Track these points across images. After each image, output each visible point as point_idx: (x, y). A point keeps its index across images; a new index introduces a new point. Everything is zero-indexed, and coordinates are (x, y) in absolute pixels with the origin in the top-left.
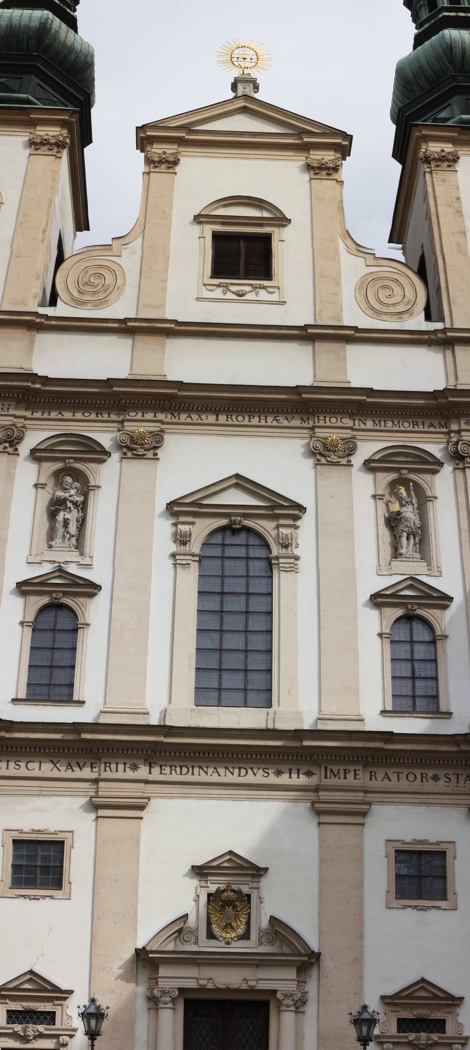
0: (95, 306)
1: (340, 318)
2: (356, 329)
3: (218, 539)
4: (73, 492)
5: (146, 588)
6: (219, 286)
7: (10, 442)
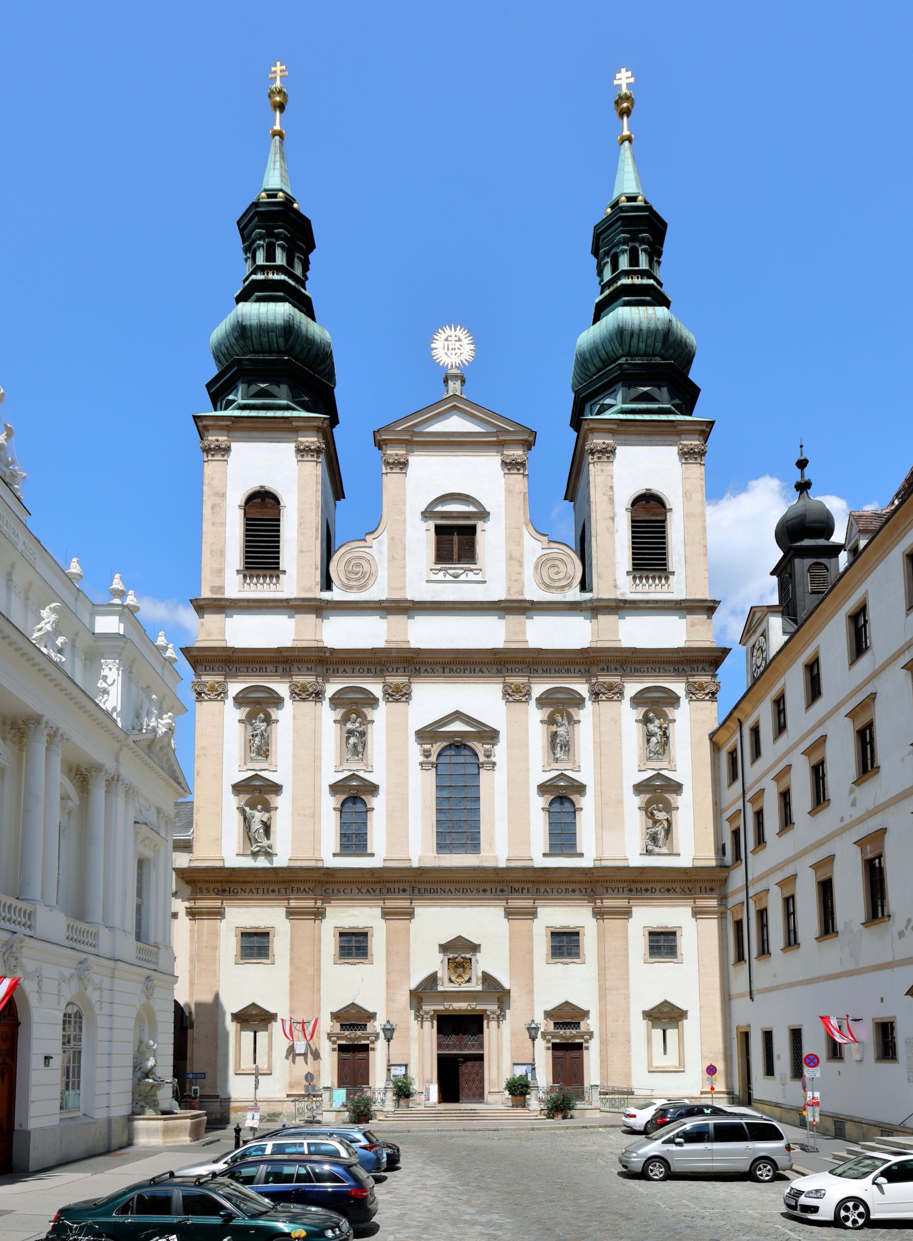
0: (358, 589)
1: (522, 594)
2: (532, 602)
3: (448, 753)
4: (357, 725)
5: (405, 785)
6: (440, 570)
7: (316, 694)
